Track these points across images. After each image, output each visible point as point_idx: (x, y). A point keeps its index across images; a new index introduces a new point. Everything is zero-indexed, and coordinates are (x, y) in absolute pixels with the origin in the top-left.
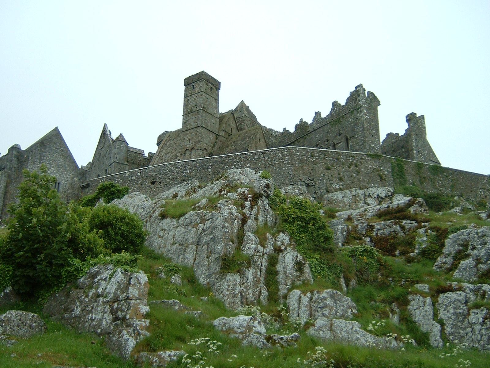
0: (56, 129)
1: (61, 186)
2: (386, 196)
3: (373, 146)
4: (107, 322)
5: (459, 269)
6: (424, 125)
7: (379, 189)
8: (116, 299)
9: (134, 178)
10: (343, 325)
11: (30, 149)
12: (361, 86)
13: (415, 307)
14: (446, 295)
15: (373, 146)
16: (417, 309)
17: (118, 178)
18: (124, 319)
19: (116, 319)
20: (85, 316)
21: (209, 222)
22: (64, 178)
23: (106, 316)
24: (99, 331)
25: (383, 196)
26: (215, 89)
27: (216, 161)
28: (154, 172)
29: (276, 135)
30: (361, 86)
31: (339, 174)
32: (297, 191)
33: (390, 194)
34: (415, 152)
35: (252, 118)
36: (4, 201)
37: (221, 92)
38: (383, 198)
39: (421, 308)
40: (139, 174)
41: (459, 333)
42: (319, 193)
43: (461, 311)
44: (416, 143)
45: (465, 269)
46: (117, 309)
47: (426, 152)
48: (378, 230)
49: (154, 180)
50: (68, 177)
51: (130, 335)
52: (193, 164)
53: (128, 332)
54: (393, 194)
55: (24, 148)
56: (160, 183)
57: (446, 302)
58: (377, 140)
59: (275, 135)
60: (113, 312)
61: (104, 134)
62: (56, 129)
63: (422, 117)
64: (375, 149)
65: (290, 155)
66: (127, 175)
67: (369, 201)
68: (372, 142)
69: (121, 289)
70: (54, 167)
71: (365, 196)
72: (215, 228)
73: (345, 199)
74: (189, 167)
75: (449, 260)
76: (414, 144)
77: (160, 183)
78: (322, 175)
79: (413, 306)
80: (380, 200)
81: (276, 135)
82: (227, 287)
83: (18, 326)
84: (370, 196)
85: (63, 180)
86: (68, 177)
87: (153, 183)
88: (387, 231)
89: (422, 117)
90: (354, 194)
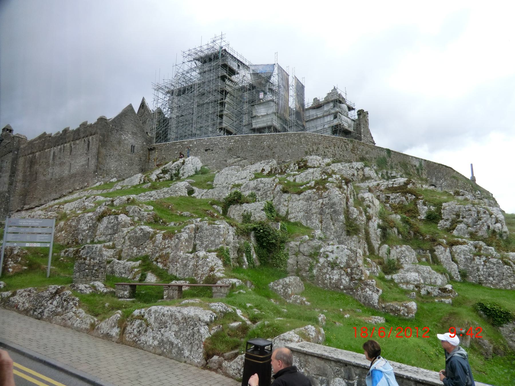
1: (135, 148)
4: (346, 282)
5: (457, 230)
8: (348, 266)
9: (191, 145)
10: (425, 269)
11: (114, 121)
13: (439, 253)
14: (457, 246)
16: (441, 254)
17: (179, 145)
18: (360, 279)
19: (352, 279)
20: (322, 276)
21: (327, 199)
23: (343, 277)
24: (342, 287)
25: (359, 168)
27: (253, 138)
28: (207, 142)
36: (98, 159)
38: (359, 169)
39: (444, 254)
40: (195, 143)
41: (469, 269)
43: (469, 257)
45: (461, 230)
46: (352, 273)
48: (392, 199)
49: (207, 148)
50: (140, 141)
51: (373, 291)
53: (370, 290)
56: (212, 150)
57: (458, 251)
61: (143, 106)
66: (186, 143)
69: (352, 260)
70: (130, 134)
72: (334, 204)
74: (233, 141)
75: (448, 223)
77: (212, 150)
79: (438, 252)
82: (354, 245)
83: (296, 287)
86: (140, 141)
87: (206, 150)
88: (398, 200)
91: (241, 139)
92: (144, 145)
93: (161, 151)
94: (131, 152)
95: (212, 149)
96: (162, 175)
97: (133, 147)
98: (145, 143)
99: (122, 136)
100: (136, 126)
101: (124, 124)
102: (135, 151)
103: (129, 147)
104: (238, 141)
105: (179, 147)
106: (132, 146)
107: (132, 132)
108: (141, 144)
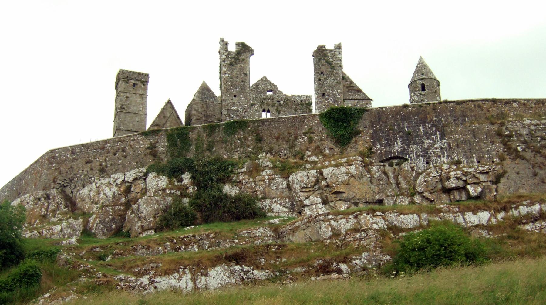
3: (236, 108)
7: (126, 173)
15: (236, 108)
26: (139, 83)
29: (301, 101)
31: (101, 165)
33: (141, 175)
35: (273, 88)
37: (150, 86)
47: (339, 91)
54: (146, 175)
58: (243, 99)
59: (299, 101)
63: (339, 47)
64: (238, 111)
68: (234, 104)
78: (80, 171)
80: (127, 184)
81: (301, 101)
90: (98, 185)
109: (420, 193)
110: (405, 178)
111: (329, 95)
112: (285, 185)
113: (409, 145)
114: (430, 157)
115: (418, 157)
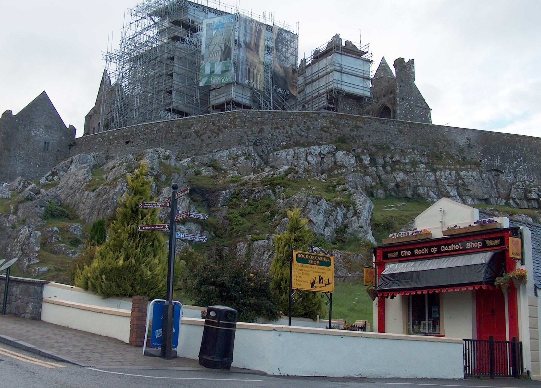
0: (44, 94)
1: (50, 144)
2: (328, 153)
6: (412, 70)
12: (337, 36)
22: (53, 137)
25: (325, 153)
30: (337, 36)
32: (240, 152)
34: (398, 99)
42: (266, 151)
44: (400, 90)
49: (128, 140)
50: (56, 136)
52: (160, 125)
55: (15, 113)
56: (133, 142)
60: (23, 250)
62: (44, 94)
65: (239, 117)
67: (310, 158)
70: (43, 129)
71: (307, 153)
73: (288, 157)
76: (398, 91)
77: (133, 142)
84: (310, 153)
85: (51, 140)
86: (56, 136)
87: (127, 143)
89: (412, 62)
91: (166, 125)
92: (62, 140)
93: (82, 146)
94: (45, 150)
95: (132, 141)
96: (51, 177)
97: (46, 143)
98: (63, 138)
99: (32, 131)
100: (51, 117)
101: (34, 117)
102: (50, 148)
103: (42, 144)
104: (162, 127)
105: (99, 141)
106: (45, 143)
107: (46, 126)
108: (58, 139)
109: (513, 199)
110: (502, 186)
111: (406, 100)
112: (433, 178)
113: (504, 163)
114: (517, 174)
115: (510, 172)
